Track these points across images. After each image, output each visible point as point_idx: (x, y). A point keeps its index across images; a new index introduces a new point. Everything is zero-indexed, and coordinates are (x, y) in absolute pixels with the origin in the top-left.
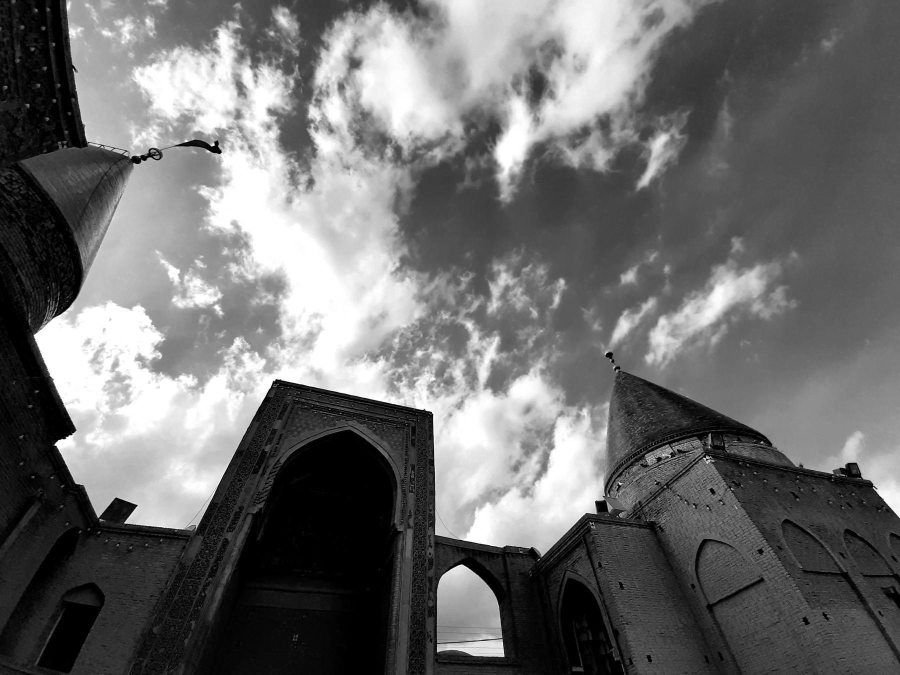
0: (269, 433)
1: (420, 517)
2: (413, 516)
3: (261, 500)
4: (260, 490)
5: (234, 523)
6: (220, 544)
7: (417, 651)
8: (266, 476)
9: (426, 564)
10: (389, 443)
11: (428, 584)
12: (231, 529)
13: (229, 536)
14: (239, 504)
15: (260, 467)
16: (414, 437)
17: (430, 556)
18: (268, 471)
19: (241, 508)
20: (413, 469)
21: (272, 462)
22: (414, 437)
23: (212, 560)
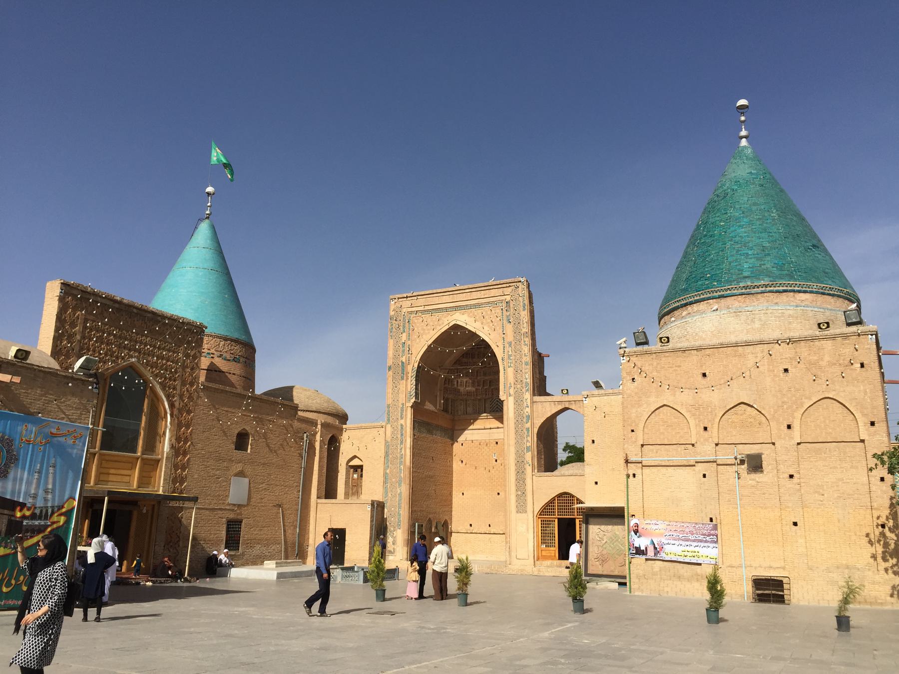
0: (401, 346)
1: (519, 386)
2: (513, 388)
3: (412, 397)
4: (409, 390)
5: (402, 414)
6: (399, 427)
7: (521, 472)
8: (409, 380)
9: (525, 420)
10: (489, 326)
11: (526, 433)
12: (402, 418)
13: (402, 422)
14: (401, 402)
15: (403, 374)
16: (508, 313)
17: (527, 414)
18: (410, 375)
19: (403, 404)
20: (510, 344)
21: (410, 368)
22: (508, 313)
23: (399, 436)
